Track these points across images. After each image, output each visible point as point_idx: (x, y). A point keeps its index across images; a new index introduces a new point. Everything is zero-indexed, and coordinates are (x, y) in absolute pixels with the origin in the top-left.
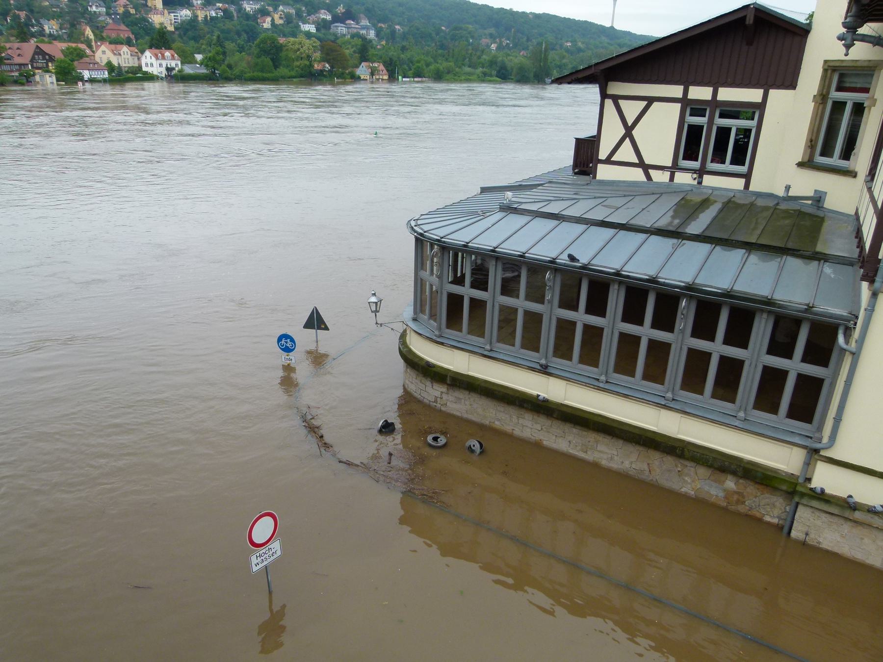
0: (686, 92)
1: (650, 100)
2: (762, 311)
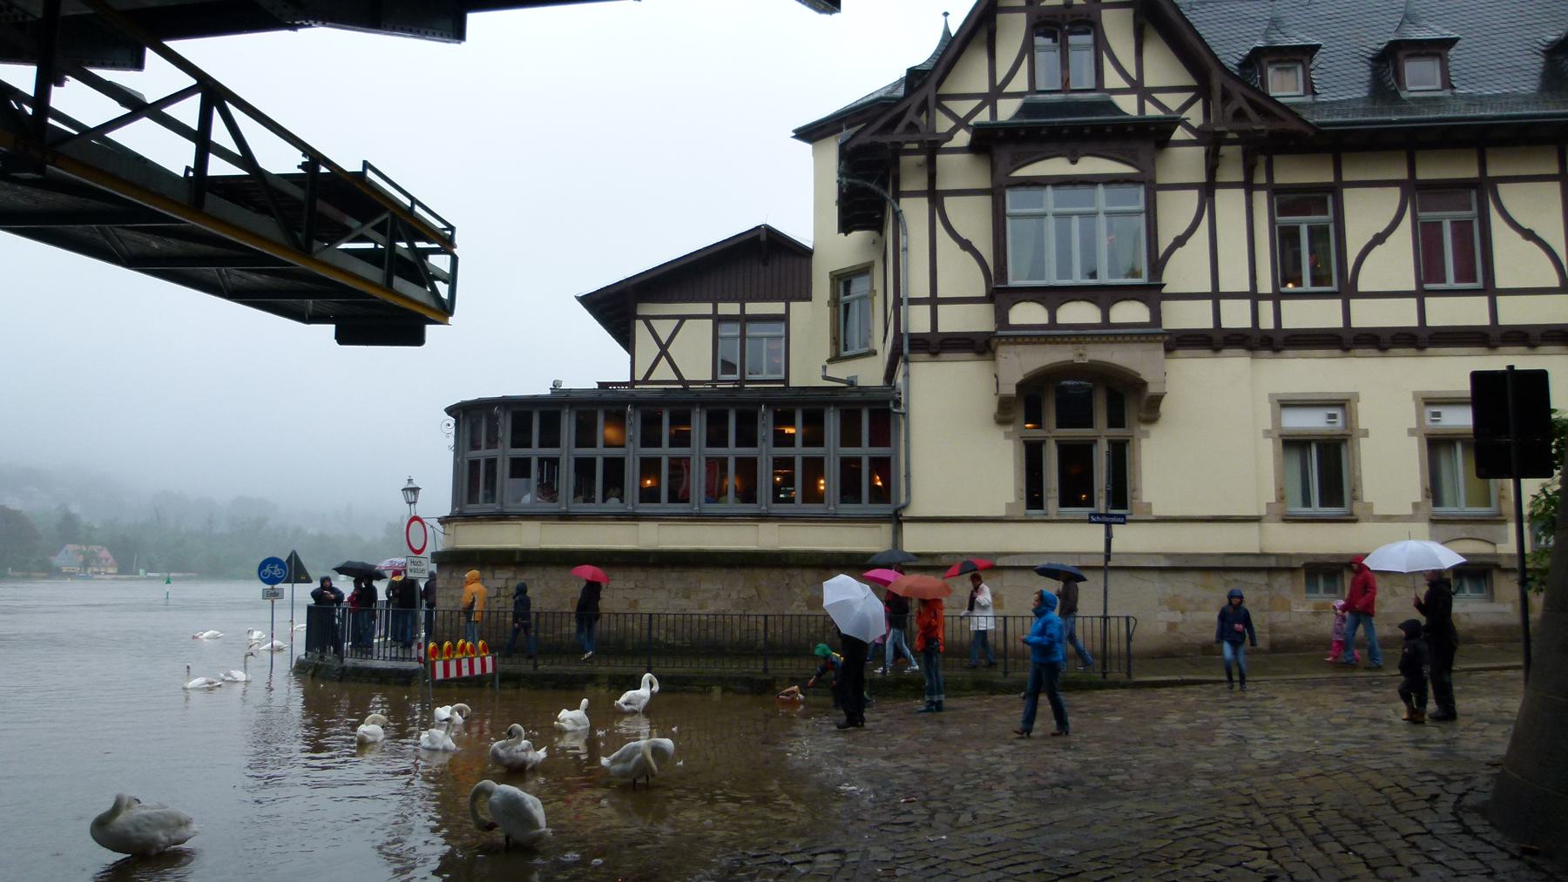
0: (715, 308)
1: (682, 319)
2: (828, 403)
